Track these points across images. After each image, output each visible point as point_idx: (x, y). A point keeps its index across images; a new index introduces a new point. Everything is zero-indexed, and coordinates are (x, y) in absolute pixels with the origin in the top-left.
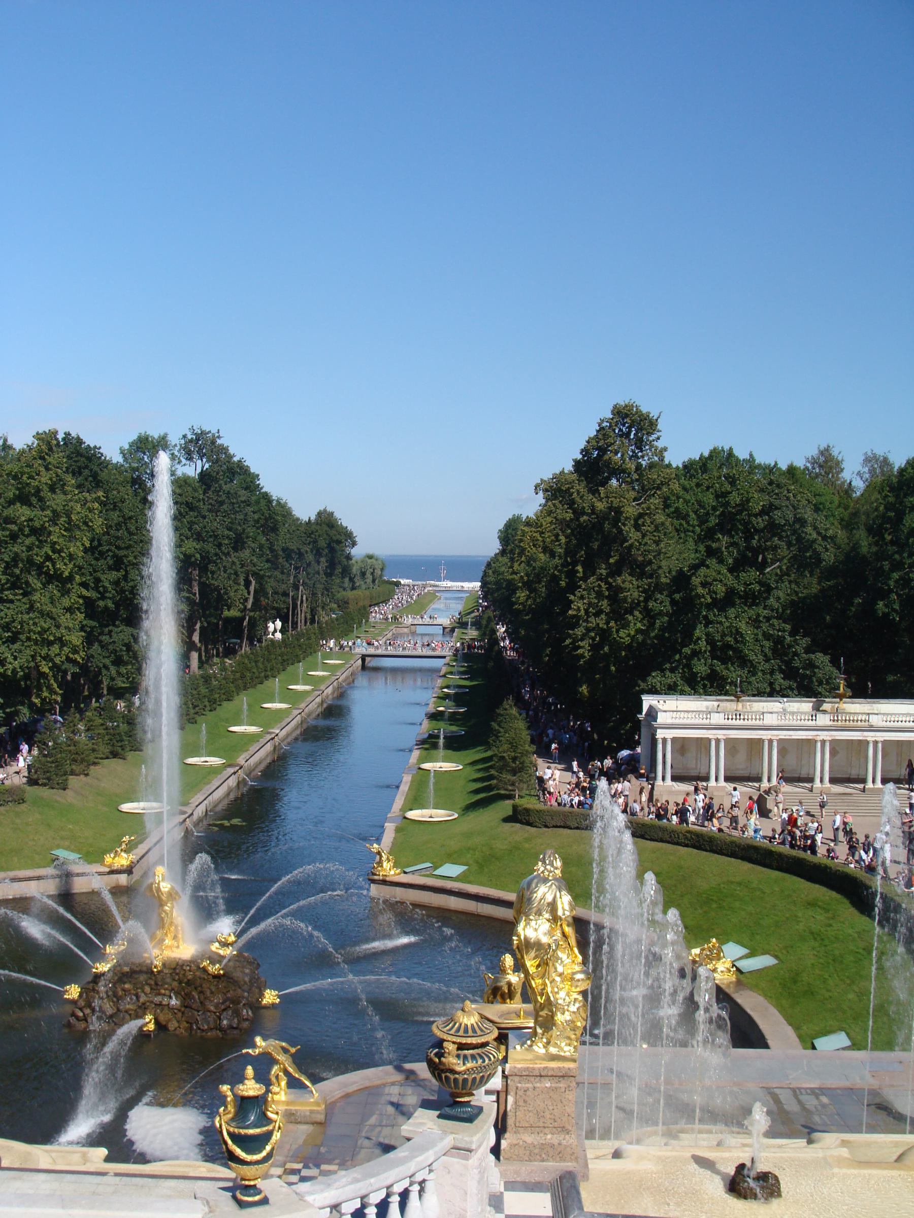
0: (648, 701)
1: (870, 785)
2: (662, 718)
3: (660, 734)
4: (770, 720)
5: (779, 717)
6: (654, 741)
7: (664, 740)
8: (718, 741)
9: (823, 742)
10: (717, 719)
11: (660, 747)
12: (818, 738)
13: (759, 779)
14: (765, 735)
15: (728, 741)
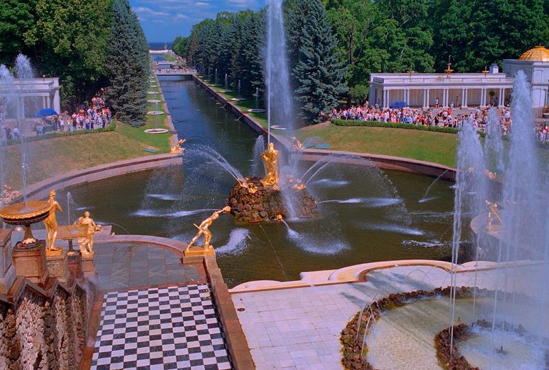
0: (373, 76)
1: (463, 107)
2: (385, 82)
3: (385, 88)
4: (427, 82)
5: (429, 80)
6: (383, 91)
7: (387, 91)
8: (407, 90)
9: (446, 90)
10: (407, 82)
11: (385, 93)
12: (464, 88)
13: (422, 106)
14: (425, 88)
15: (411, 90)
